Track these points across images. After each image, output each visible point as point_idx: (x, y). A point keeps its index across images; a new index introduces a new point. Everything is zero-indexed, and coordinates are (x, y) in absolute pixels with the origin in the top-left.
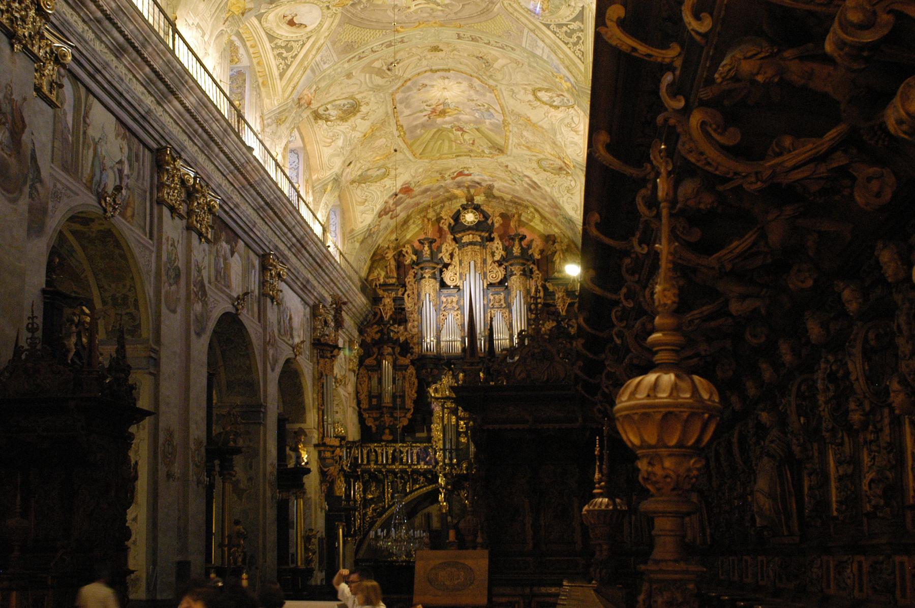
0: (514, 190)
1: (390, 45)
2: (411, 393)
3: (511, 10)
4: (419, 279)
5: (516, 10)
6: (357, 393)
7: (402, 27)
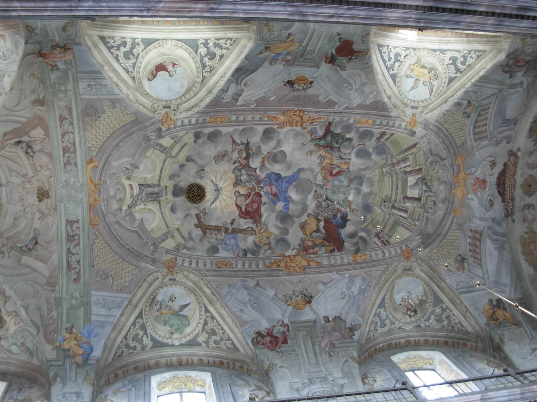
1: (66, 150)
3: (150, 279)
5: (150, 285)
7: (96, 167)
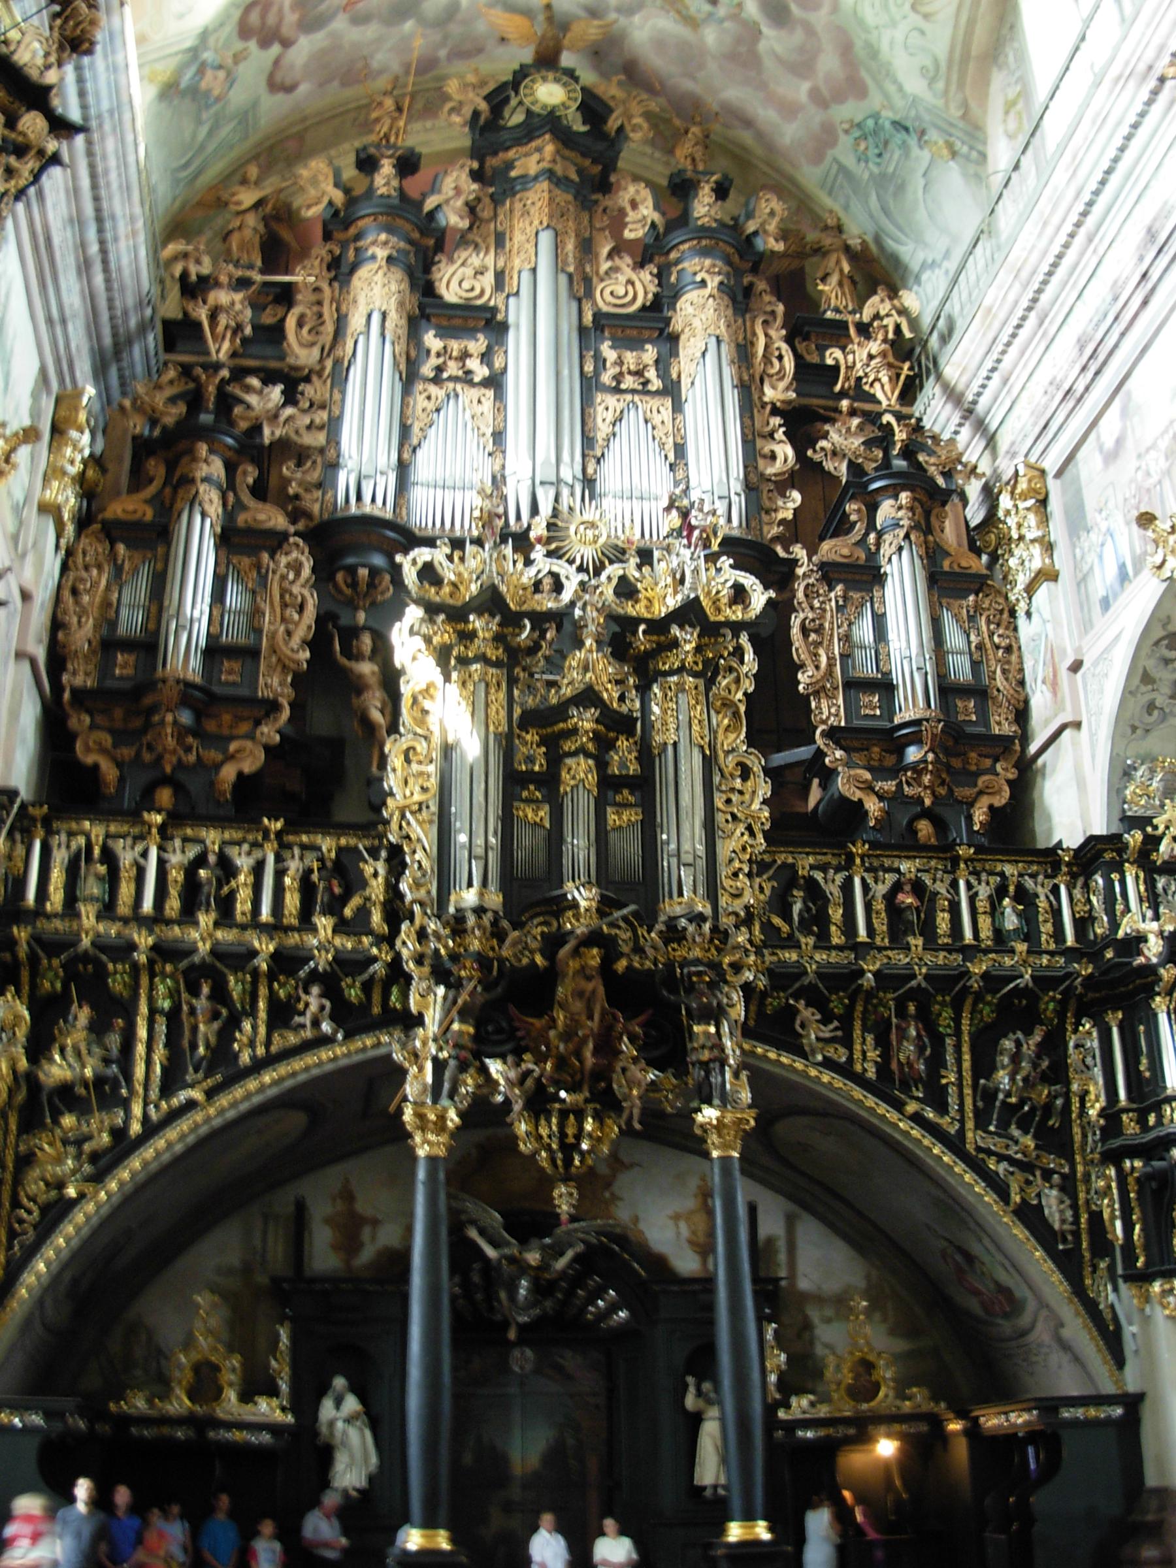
0: (691, 57)
2: (292, 638)
4: (341, 271)
6: (56, 625)
